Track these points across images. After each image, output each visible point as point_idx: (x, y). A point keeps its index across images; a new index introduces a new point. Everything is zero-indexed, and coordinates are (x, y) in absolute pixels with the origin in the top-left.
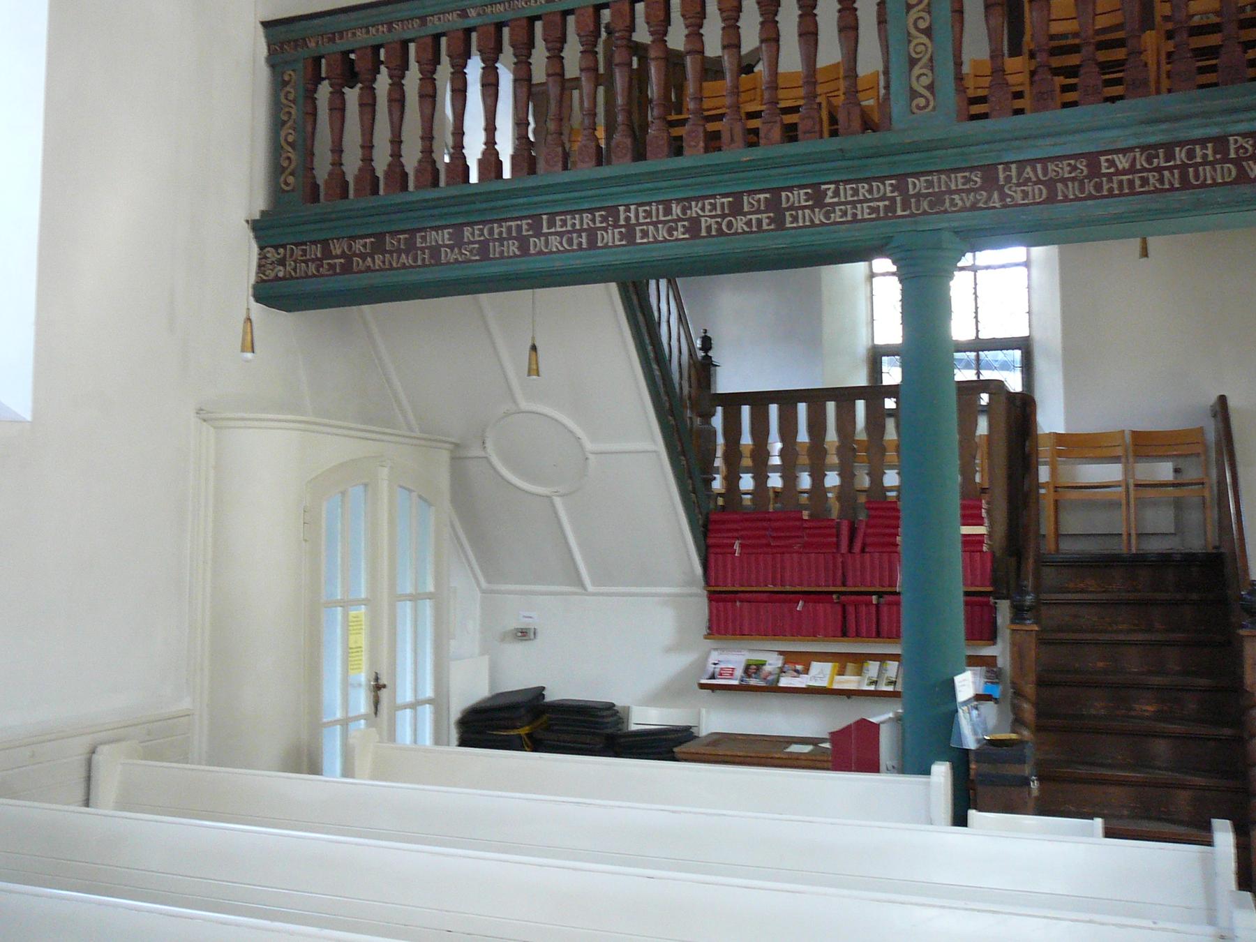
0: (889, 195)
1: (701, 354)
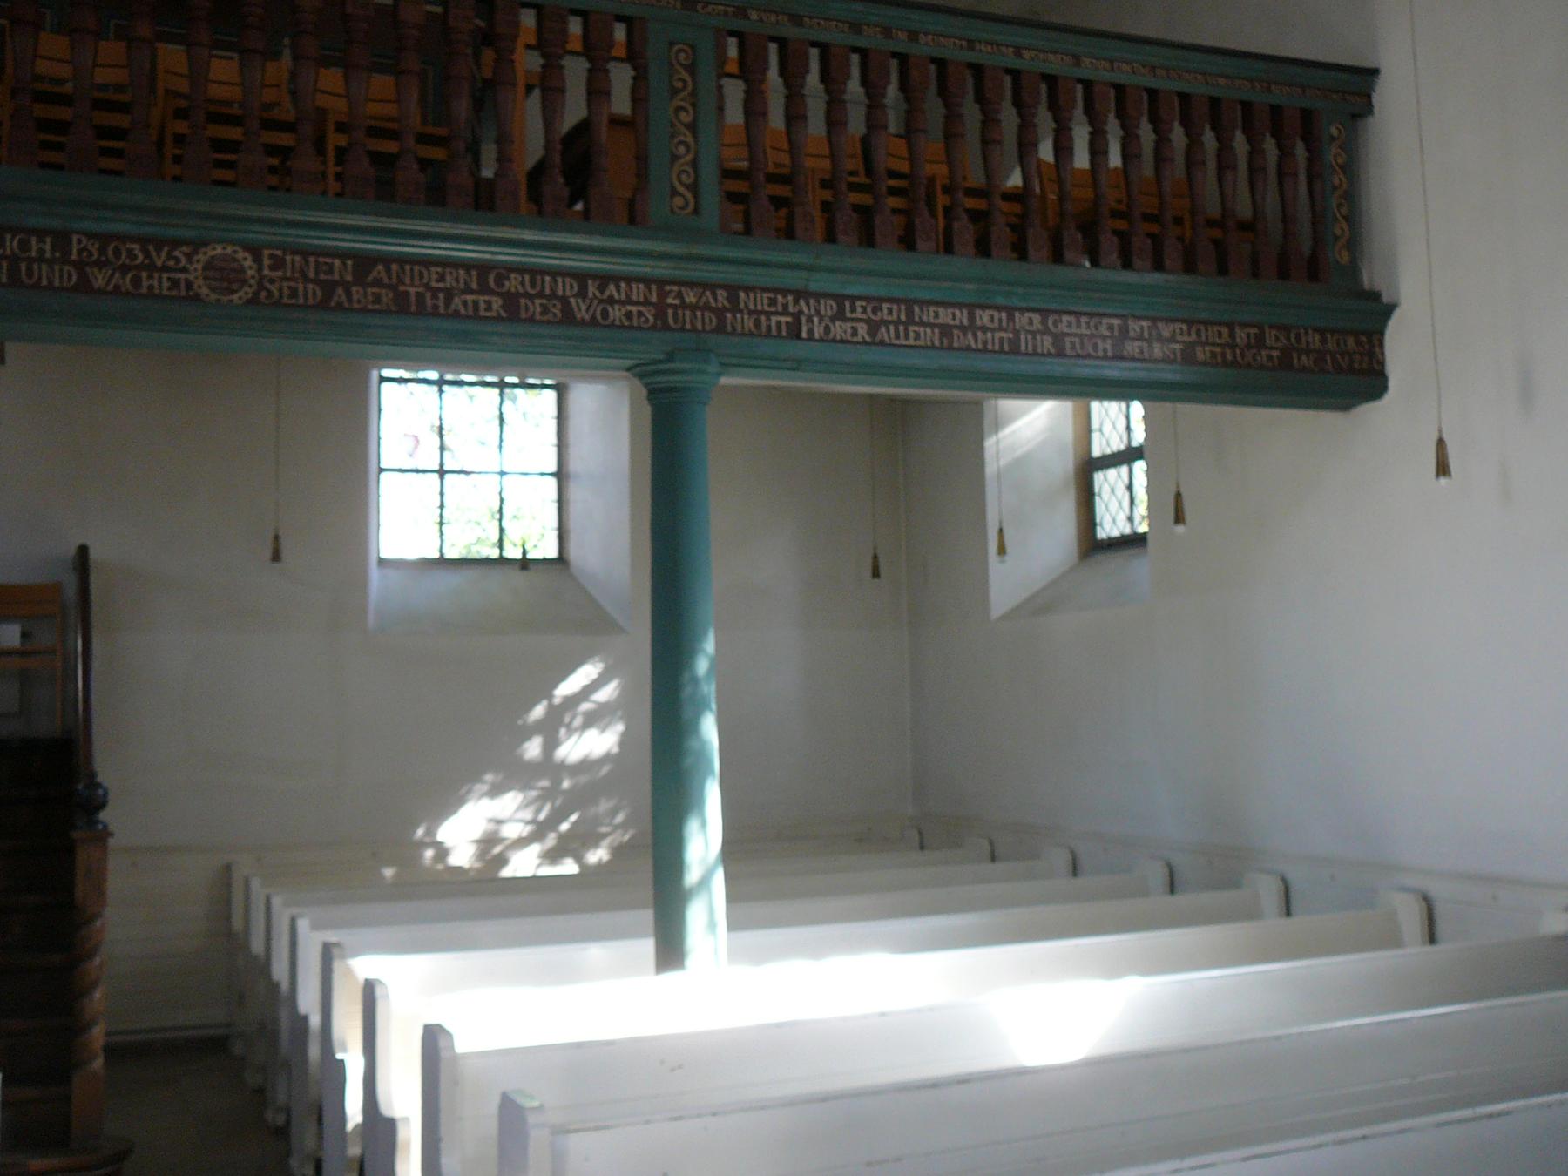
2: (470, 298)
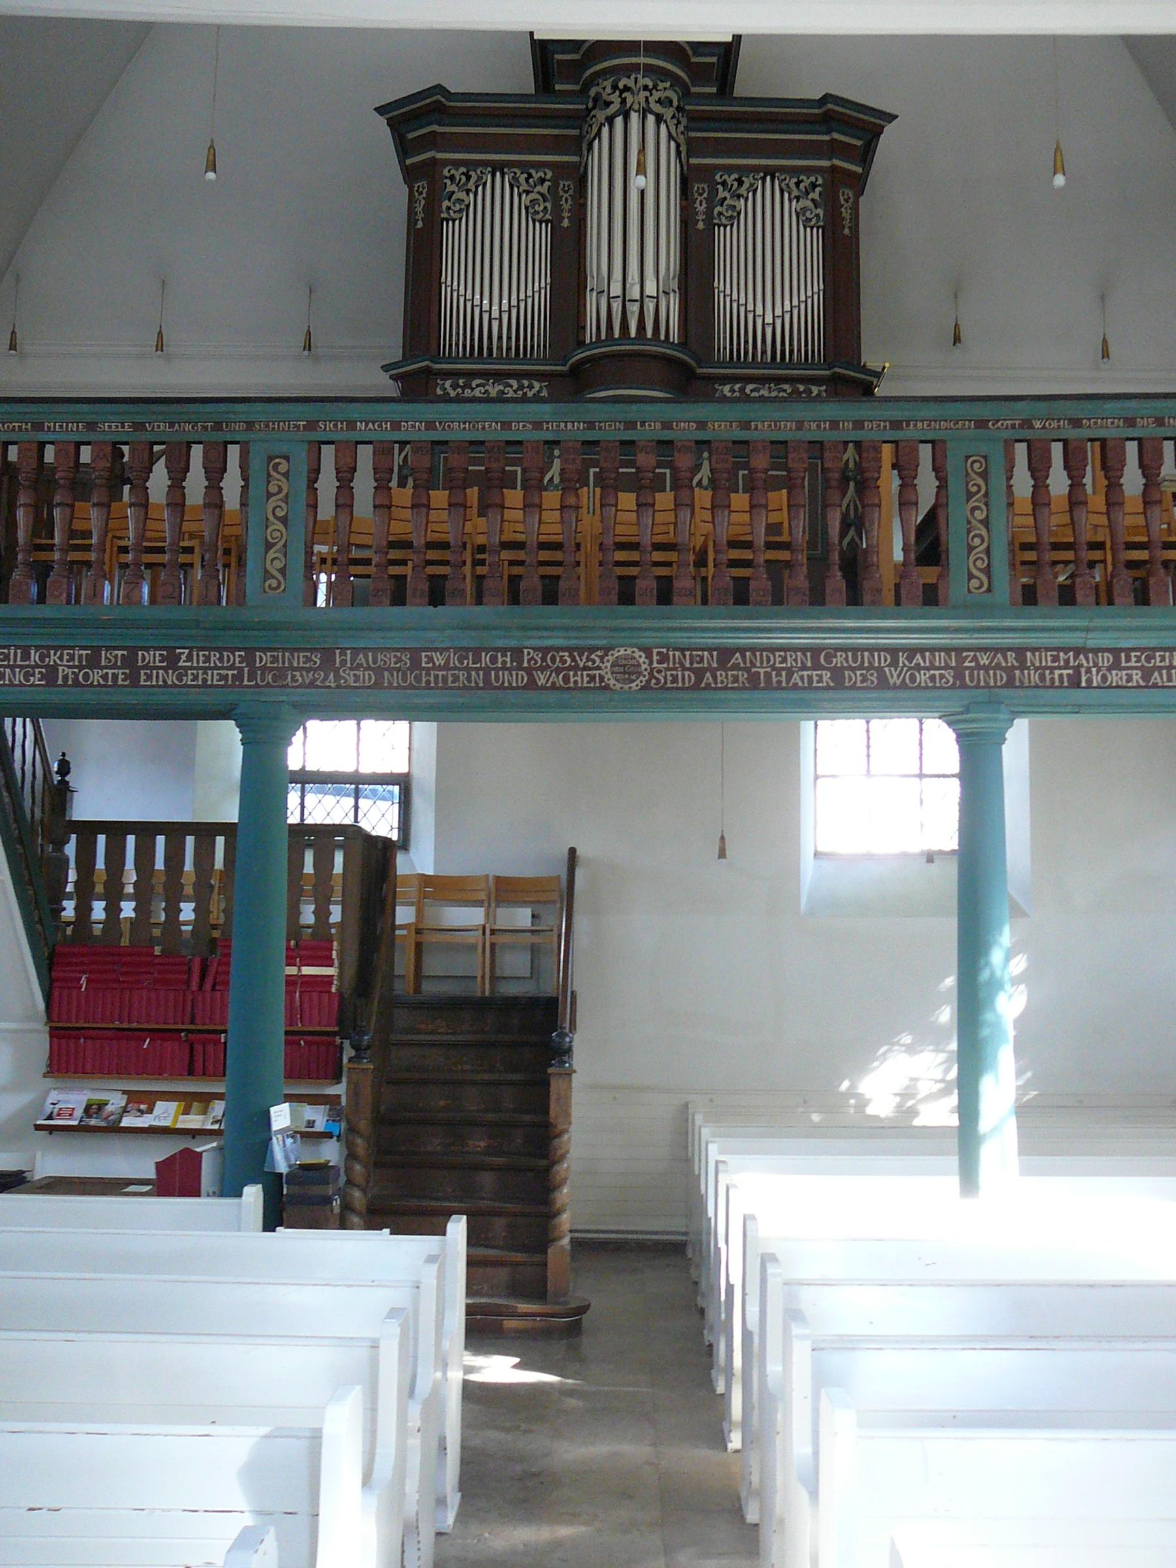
0: (237, 665)
1: (57, 778)
2: (805, 673)
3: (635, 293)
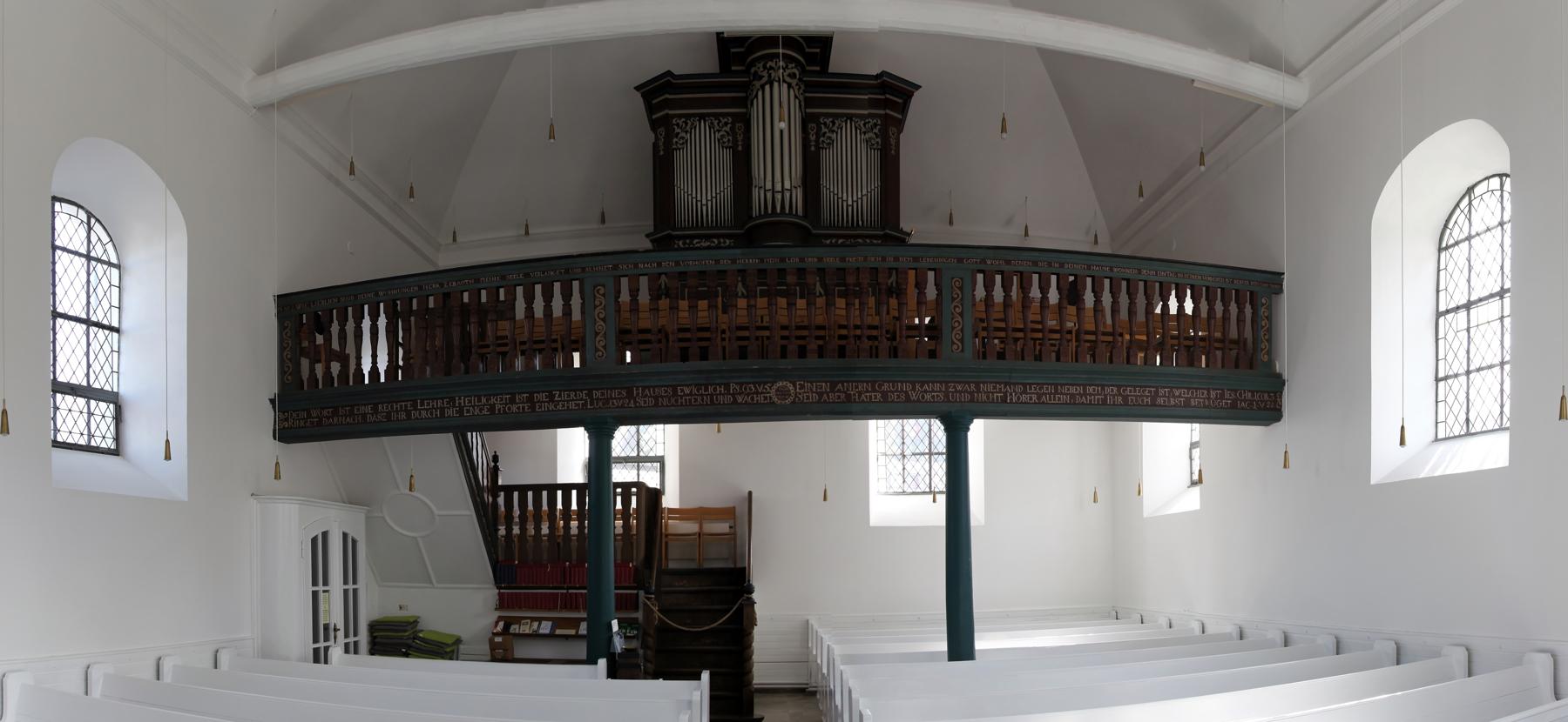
3: (778, 187)
